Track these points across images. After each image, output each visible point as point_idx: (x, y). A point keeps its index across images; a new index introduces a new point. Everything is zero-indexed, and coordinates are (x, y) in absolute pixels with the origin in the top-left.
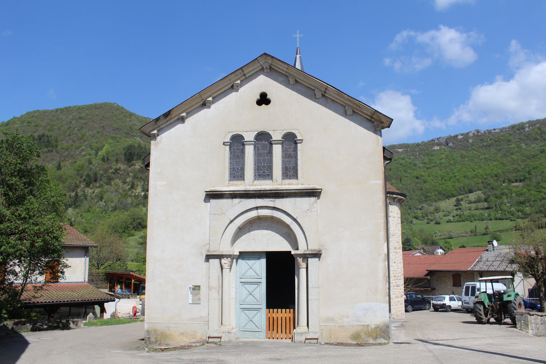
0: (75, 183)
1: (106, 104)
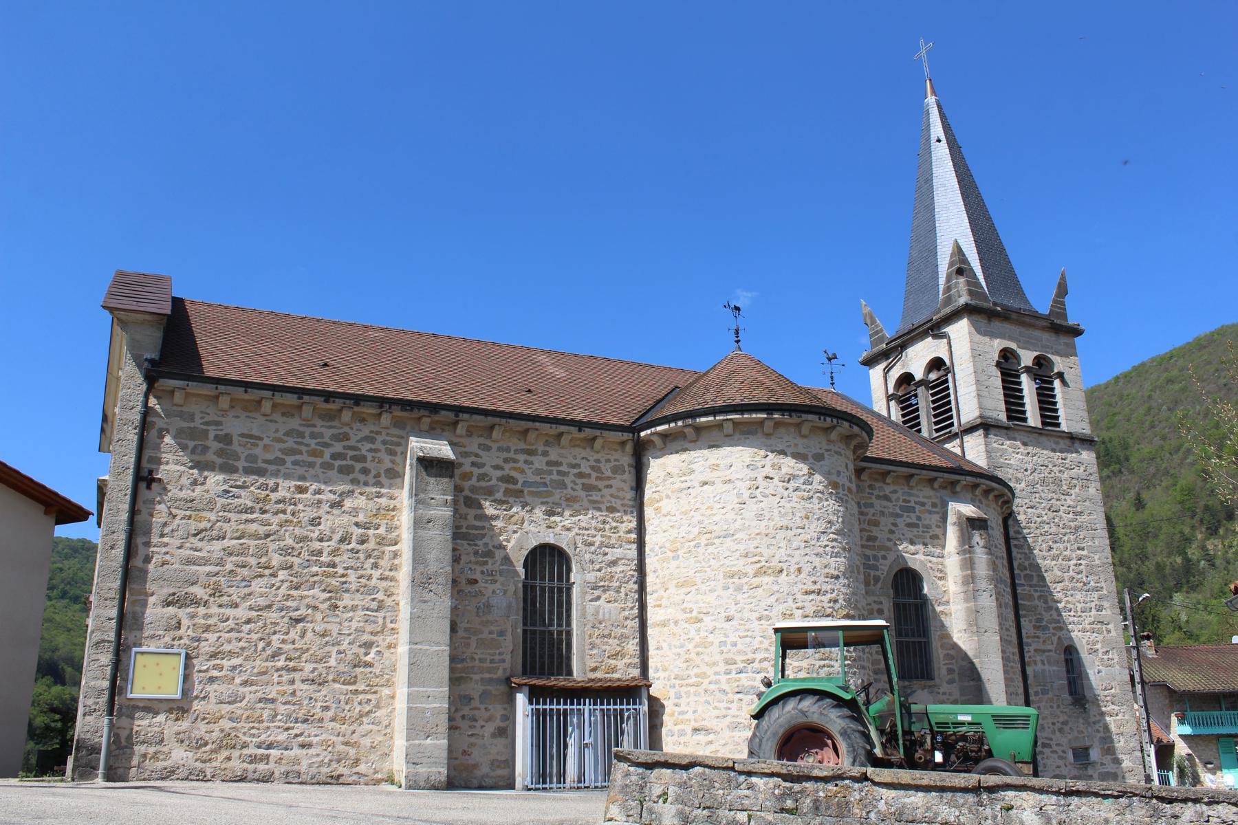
0: (1182, 532)
1: (1222, 332)
